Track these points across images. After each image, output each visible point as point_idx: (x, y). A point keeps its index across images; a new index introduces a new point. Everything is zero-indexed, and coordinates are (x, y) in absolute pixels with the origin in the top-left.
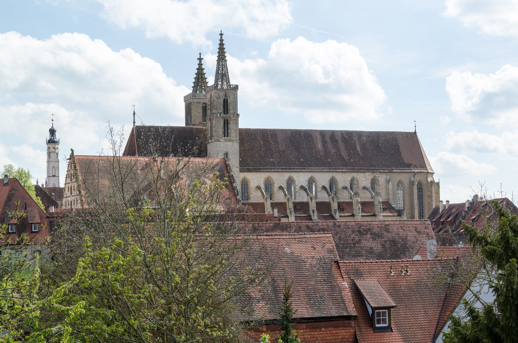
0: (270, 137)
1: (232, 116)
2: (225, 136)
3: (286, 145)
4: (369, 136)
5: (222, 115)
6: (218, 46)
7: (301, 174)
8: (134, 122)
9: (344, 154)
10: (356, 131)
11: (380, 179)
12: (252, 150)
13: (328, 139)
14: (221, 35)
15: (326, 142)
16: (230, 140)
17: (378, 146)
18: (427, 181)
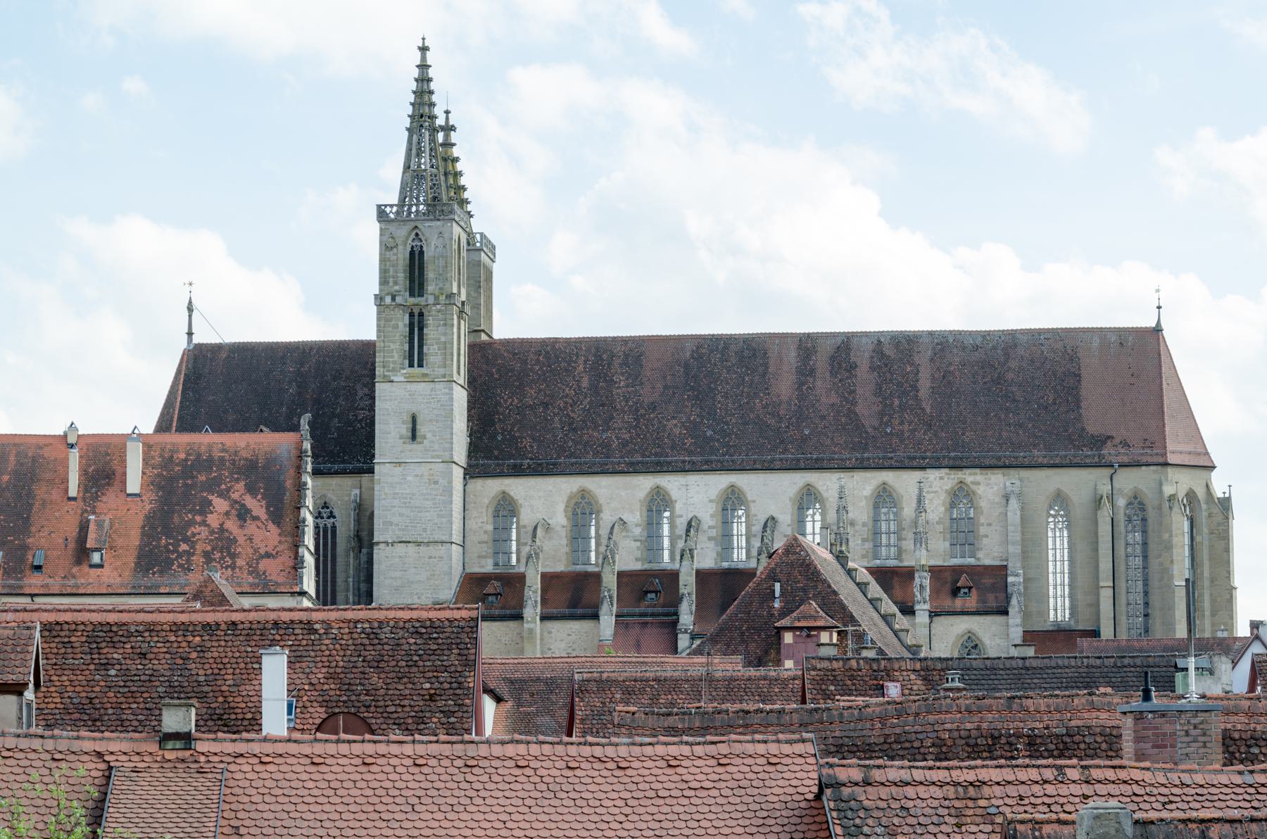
0: (617, 362)
1: (431, 300)
2: (411, 365)
3: (666, 387)
4: (976, 348)
5: (399, 300)
6: (414, 86)
7: (693, 479)
8: (190, 334)
9: (866, 409)
10: (931, 333)
11: (980, 490)
12: (546, 405)
13: (821, 362)
14: (424, 49)
15: (812, 372)
16: (426, 375)
17: (998, 380)
18: (1161, 492)
